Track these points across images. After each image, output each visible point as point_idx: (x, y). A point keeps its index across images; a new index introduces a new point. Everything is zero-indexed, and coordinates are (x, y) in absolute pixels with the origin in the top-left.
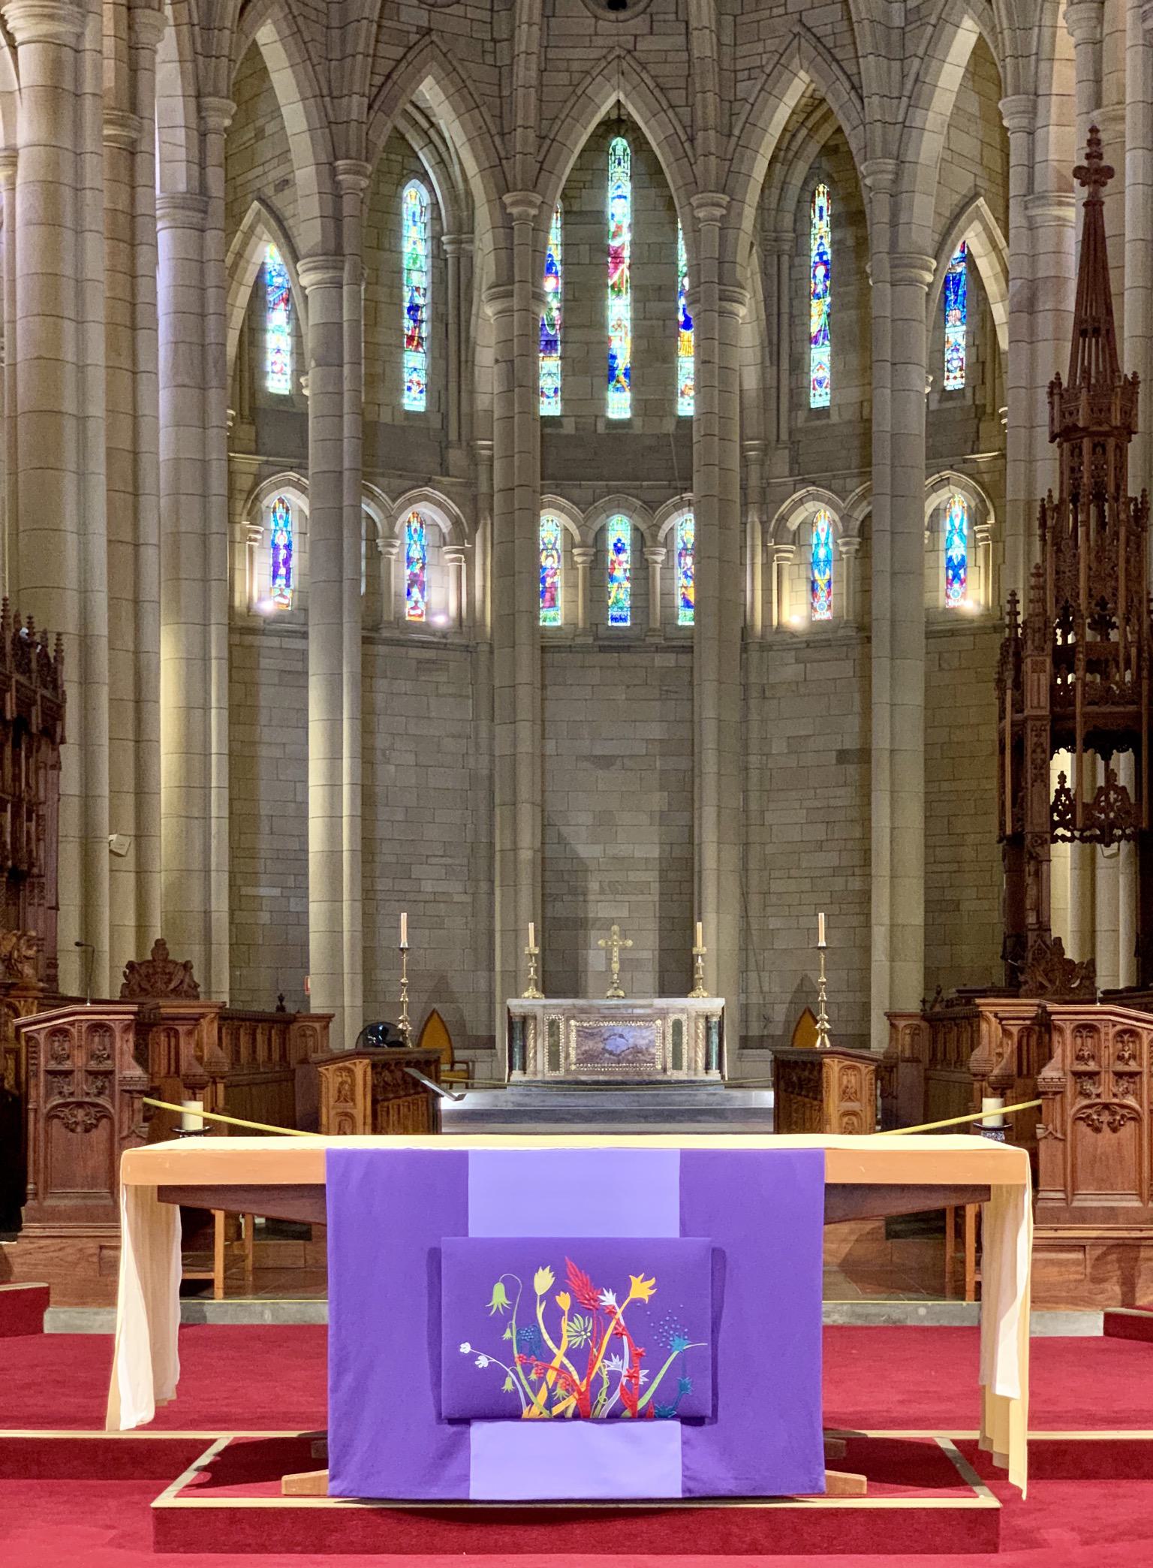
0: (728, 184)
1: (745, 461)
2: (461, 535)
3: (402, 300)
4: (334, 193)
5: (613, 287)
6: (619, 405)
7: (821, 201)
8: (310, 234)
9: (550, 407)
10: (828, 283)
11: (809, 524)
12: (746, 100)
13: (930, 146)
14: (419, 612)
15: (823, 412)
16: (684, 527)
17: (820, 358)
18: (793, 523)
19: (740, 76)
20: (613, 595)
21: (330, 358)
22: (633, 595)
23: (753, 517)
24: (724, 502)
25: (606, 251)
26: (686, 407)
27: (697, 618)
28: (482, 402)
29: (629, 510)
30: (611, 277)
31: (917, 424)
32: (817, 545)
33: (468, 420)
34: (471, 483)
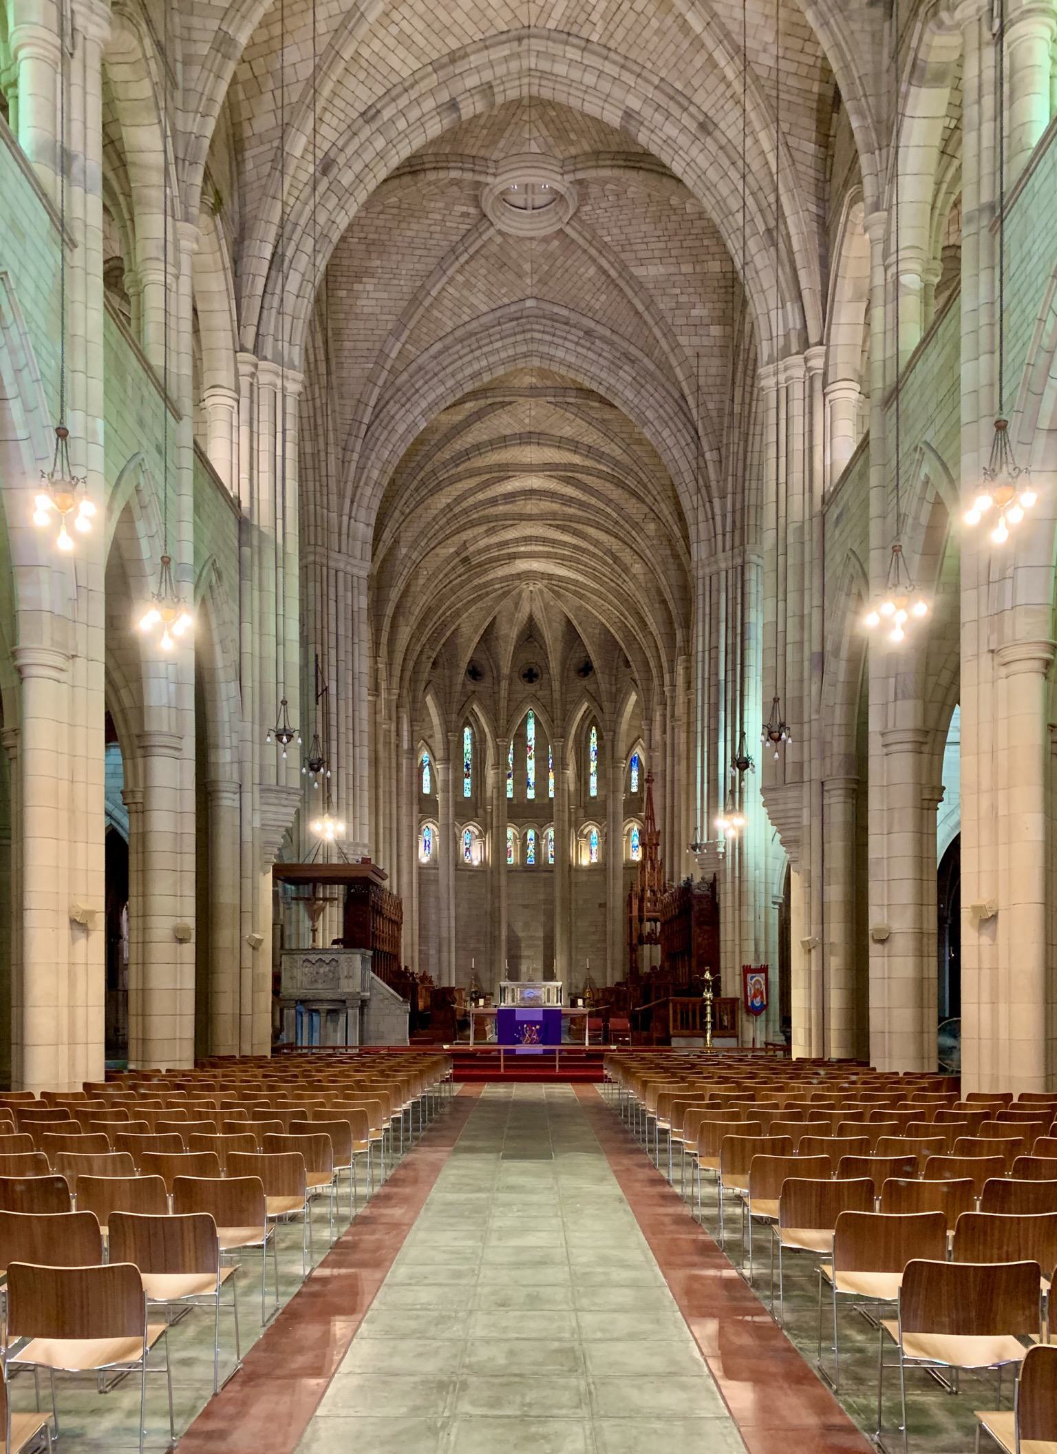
0: (564, 736)
1: (570, 813)
2: (481, 836)
4: (447, 742)
6: (531, 794)
7: (594, 731)
8: (440, 753)
9: (510, 795)
11: (590, 832)
13: (624, 727)
15: (595, 798)
16: (551, 833)
17: (593, 781)
18: (585, 832)
21: (445, 790)
23: (573, 830)
24: (563, 830)
26: (551, 795)
28: (489, 794)
29: (533, 828)
31: (620, 809)
33: (484, 799)
34: (485, 819)
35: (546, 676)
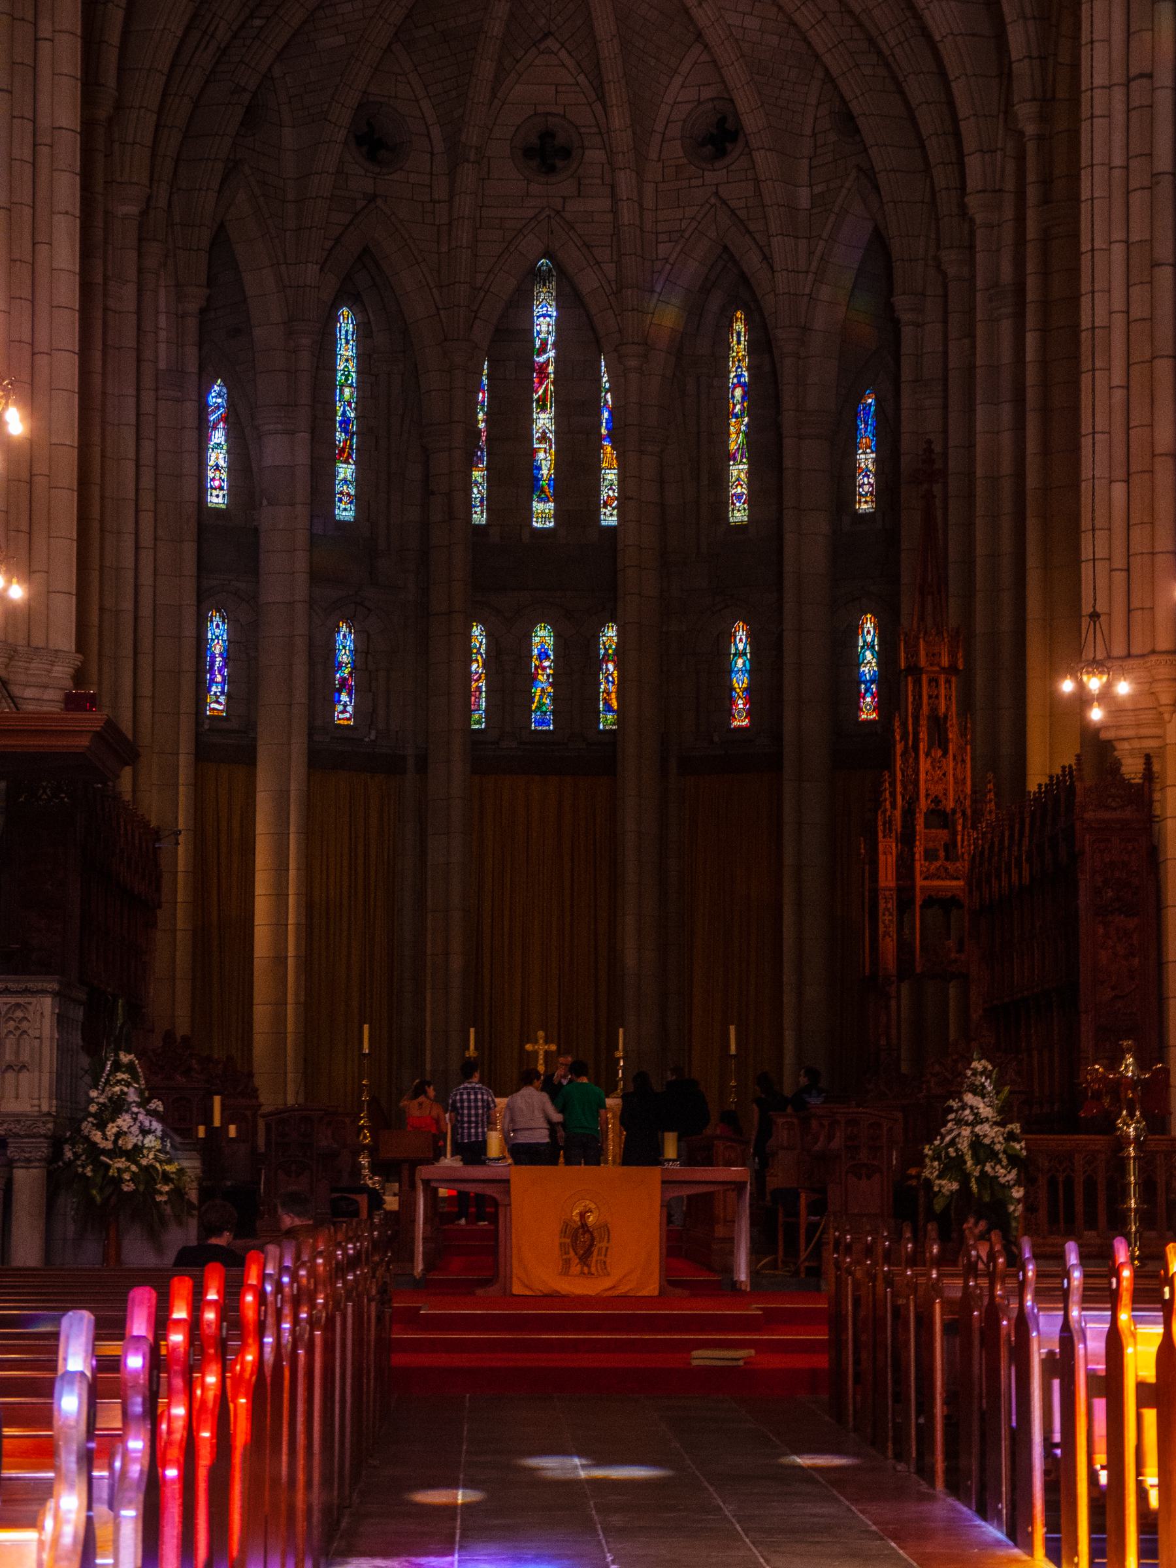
3: (335, 412)
5: (538, 401)
6: (543, 514)
7: (739, 326)
9: (479, 517)
10: (745, 404)
12: (666, 260)
14: (347, 715)
15: (740, 528)
19: (661, 237)
20: (537, 698)
22: (555, 700)
25: (531, 366)
27: (618, 722)
30: (537, 392)
32: (735, 655)
35: (596, 155)
